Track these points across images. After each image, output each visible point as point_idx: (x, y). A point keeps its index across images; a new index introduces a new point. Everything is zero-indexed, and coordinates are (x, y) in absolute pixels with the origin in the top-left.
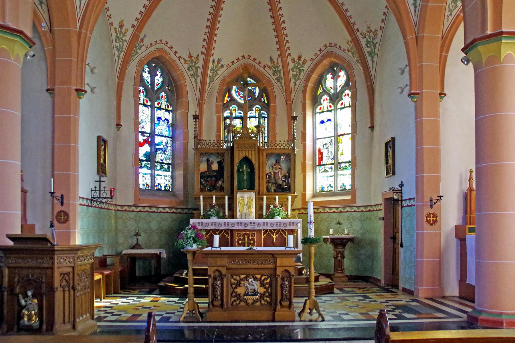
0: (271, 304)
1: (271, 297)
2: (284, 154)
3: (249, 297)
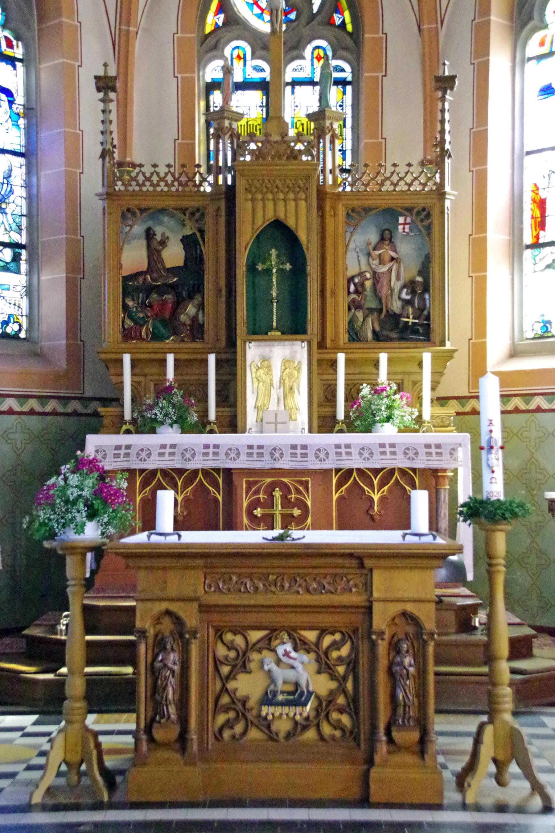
0: (356, 739)
1: (357, 712)
2: (409, 210)
3: (278, 710)
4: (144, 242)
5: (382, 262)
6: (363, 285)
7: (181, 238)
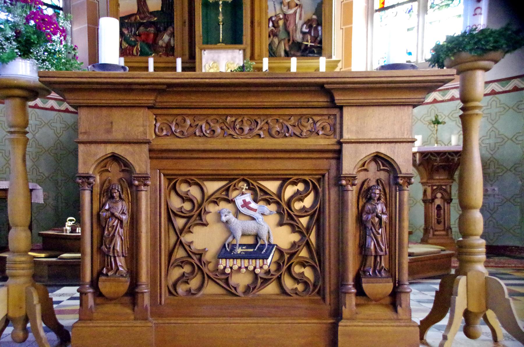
0: (321, 293)
1: (321, 263)
3: (237, 263)
5: (289, 7)
6: (277, 23)
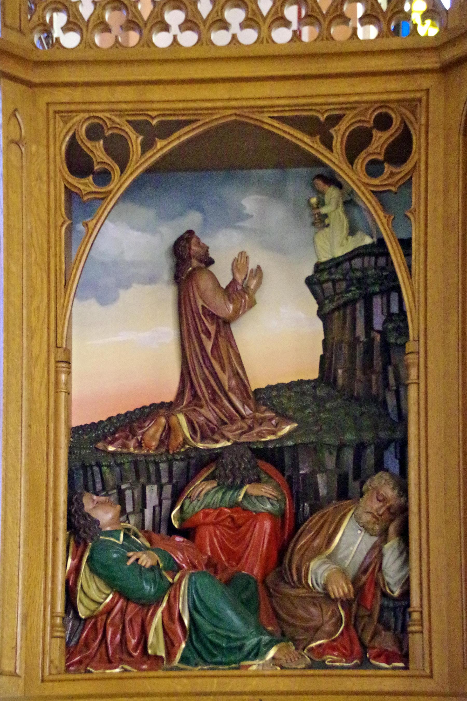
4: (168, 294)
7: (309, 272)
